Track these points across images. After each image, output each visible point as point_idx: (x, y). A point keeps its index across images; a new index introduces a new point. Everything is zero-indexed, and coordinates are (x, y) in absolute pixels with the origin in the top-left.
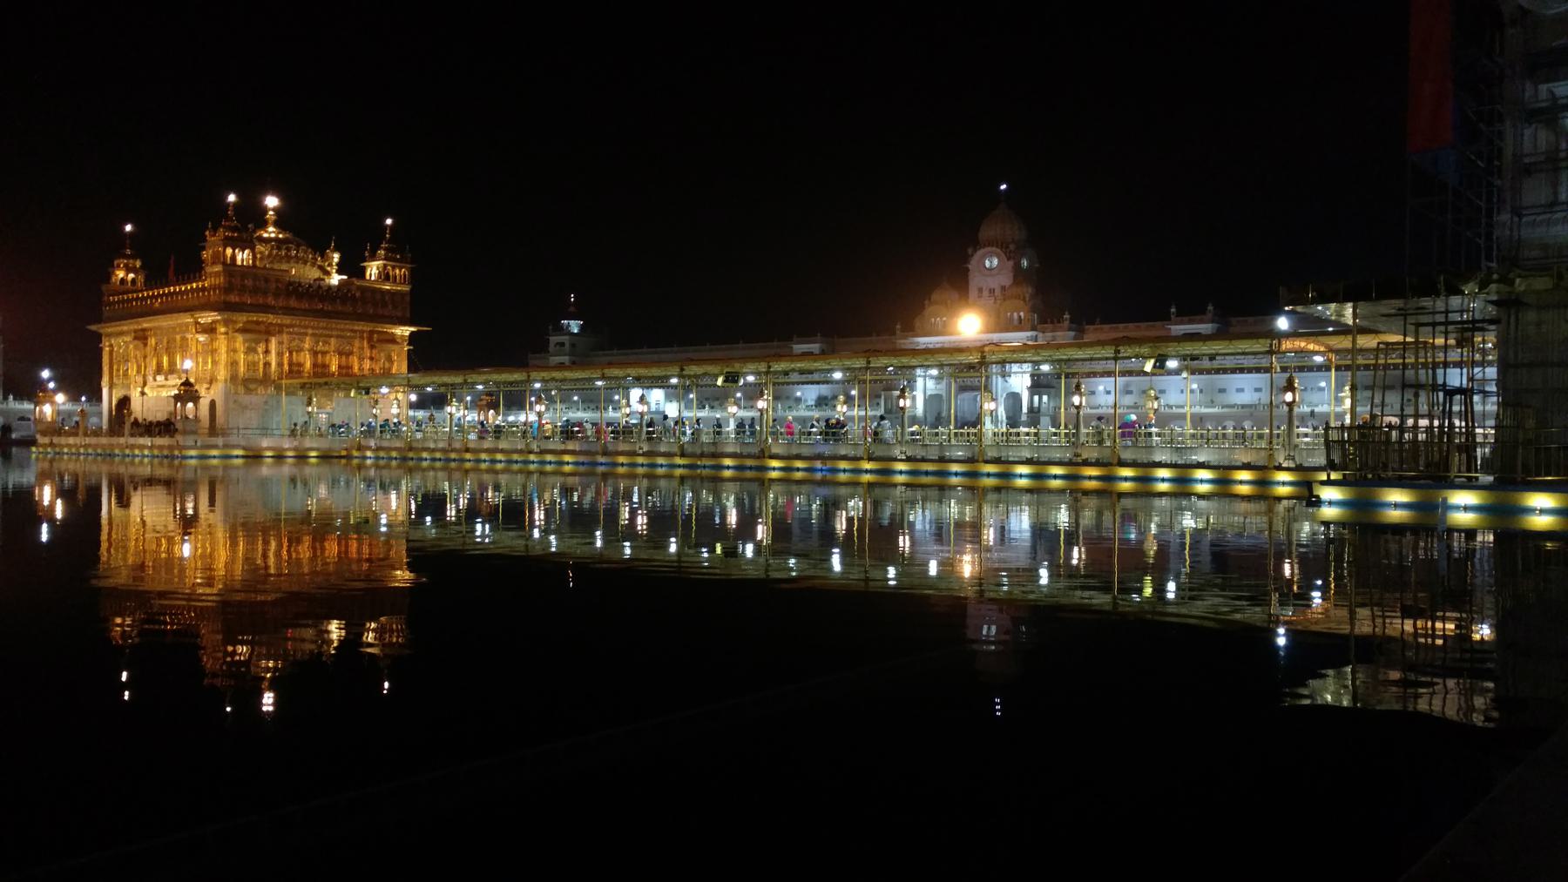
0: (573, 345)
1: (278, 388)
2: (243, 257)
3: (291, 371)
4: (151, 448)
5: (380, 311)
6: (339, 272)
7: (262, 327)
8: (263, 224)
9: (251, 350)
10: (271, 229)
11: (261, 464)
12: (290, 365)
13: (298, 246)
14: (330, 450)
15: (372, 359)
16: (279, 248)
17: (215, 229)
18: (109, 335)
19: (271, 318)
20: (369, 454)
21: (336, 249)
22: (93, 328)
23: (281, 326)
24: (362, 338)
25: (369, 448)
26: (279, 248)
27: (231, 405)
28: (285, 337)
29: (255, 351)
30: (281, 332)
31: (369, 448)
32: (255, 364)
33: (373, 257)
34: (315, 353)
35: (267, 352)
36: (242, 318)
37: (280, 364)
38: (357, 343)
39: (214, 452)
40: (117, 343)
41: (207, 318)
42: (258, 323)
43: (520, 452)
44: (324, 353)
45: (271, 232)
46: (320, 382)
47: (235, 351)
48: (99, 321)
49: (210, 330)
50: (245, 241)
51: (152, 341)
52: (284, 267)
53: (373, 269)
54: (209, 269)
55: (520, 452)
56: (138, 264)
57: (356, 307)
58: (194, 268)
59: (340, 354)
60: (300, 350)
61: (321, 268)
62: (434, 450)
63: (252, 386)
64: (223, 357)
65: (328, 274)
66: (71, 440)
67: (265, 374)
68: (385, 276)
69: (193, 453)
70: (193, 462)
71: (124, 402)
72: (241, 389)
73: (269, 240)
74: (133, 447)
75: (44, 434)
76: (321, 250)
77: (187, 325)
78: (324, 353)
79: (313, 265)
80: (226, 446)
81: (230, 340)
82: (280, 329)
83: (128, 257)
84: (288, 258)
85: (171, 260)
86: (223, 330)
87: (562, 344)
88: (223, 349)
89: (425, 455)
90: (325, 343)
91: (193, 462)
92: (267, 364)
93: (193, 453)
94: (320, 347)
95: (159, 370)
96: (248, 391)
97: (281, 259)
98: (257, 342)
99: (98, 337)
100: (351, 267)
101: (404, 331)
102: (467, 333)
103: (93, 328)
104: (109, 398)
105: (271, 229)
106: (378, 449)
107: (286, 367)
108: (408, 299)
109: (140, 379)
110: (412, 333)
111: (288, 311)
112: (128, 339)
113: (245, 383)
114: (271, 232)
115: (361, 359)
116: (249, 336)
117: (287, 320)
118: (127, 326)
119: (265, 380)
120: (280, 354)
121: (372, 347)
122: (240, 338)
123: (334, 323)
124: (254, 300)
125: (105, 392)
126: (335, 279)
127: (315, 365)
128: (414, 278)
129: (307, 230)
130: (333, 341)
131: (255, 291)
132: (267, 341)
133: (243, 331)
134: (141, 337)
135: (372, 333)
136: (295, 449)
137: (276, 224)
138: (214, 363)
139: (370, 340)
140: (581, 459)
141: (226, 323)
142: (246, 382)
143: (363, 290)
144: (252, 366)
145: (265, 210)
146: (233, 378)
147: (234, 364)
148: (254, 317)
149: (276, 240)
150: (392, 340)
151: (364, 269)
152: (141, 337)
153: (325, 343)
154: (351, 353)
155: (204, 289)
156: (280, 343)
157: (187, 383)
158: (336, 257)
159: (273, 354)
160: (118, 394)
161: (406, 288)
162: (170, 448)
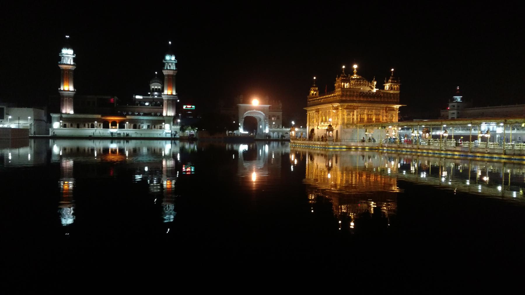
0: (458, 106)
1: (356, 126)
2: (347, 85)
3: (360, 121)
4: (320, 145)
5: (389, 100)
6: (376, 88)
7: (352, 107)
8: (352, 74)
9: (348, 115)
11: (351, 151)
12: (360, 119)
13: (363, 80)
14: (372, 147)
15: (386, 116)
17: (339, 77)
18: (309, 110)
19: (355, 104)
20: (385, 148)
22: (305, 109)
23: (358, 106)
24: (383, 109)
25: (385, 147)
26: (357, 81)
28: (359, 110)
29: (350, 115)
30: (357, 108)
31: (385, 147)
32: (349, 119)
33: (387, 82)
34: (368, 115)
35: (353, 115)
36: (346, 105)
37: (357, 119)
38: (381, 111)
39: (337, 147)
40: (311, 113)
41: (336, 105)
42: (351, 106)
43: (438, 150)
45: (355, 76)
46: (369, 124)
47: (344, 115)
48: (306, 106)
49: (337, 109)
50: (347, 81)
51: (320, 112)
52: (359, 87)
53: (387, 86)
54: (337, 90)
55: (438, 150)
56: (317, 89)
57: (381, 99)
58: (332, 89)
59: (376, 115)
60: (363, 114)
61: (371, 87)
62: (407, 148)
63: (349, 126)
64: (340, 117)
65: (372, 88)
66: (299, 142)
67: (353, 122)
68: (391, 88)
69: (331, 147)
70: (331, 150)
71: (313, 130)
72: (345, 127)
73: (355, 79)
74: (315, 144)
75: (292, 139)
76: (370, 81)
77: (330, 107)
79: (368, 86)
80: (341, 145)
81: (343, 112)
82: (357, 107)
83: (314, 87)
84: (360, 84)
85: (326, 88)
86: (340, 108)
87: (454, 106)
88: (340, 115)
89: (404, 150)
90: (371, 111)
91: (331, 150)
92: (353, 119)
93: (331, 147)
94: (370, 113)
95: (322, 121)
96: (348, 127)
97: (358, 85)
98: (350, 112)
99: (306, 111)
100: (380, 86)
101: (397, 106)
102: (419, 107)
103: (305, 109)
104: (308, 129)
105: (355, 75)
106: (388, 147)
107: (359, 120)
108: (399, 95)
109: (317, 124)
110: (400, 107)
111: (360, 102)
112: (314, 112)
113: (347, 125)
114: (355, 76)
115: (383, 116)
116: (348, 110)
117: (359, 105)
118: (313, 108)
119: (353, 124)
120: (357, 115)
121: (386, 112)
122: (345, 111)
123: (374, 105)
124: (350, 99)
125: (308, 127)
126: (375, 90)
127: (368, 119)
128: (401, 88)
129: (366, 75)
130: (374, 111)
131: (350, 96)
132: (353, 112)
133: (346, 109)
134: (317, 111)
135: (386, 107)
136: (361, 146)
137: (357, 74)
138: (338, 119)
139: (386, 110)
140: (462, 154)
141: (341, 106)
142: (347, 124)
143: (384, 93)
144: (348, 119)
145: (353, 69)
146: (343, 123)
147: (343, 119)
148: (350, 104)
149: (357, 79)
150: (393, 110)
151: (384, 86)
152: (317, 111)
153: (371, 111)
154: (380, 114)
155: (335, 96)
156: (357, 112)
157: (330, 126)
158: (375, 83)
159: (355, 116)
160: (311, 128)
161: (398, 92)
162: (325, 145)
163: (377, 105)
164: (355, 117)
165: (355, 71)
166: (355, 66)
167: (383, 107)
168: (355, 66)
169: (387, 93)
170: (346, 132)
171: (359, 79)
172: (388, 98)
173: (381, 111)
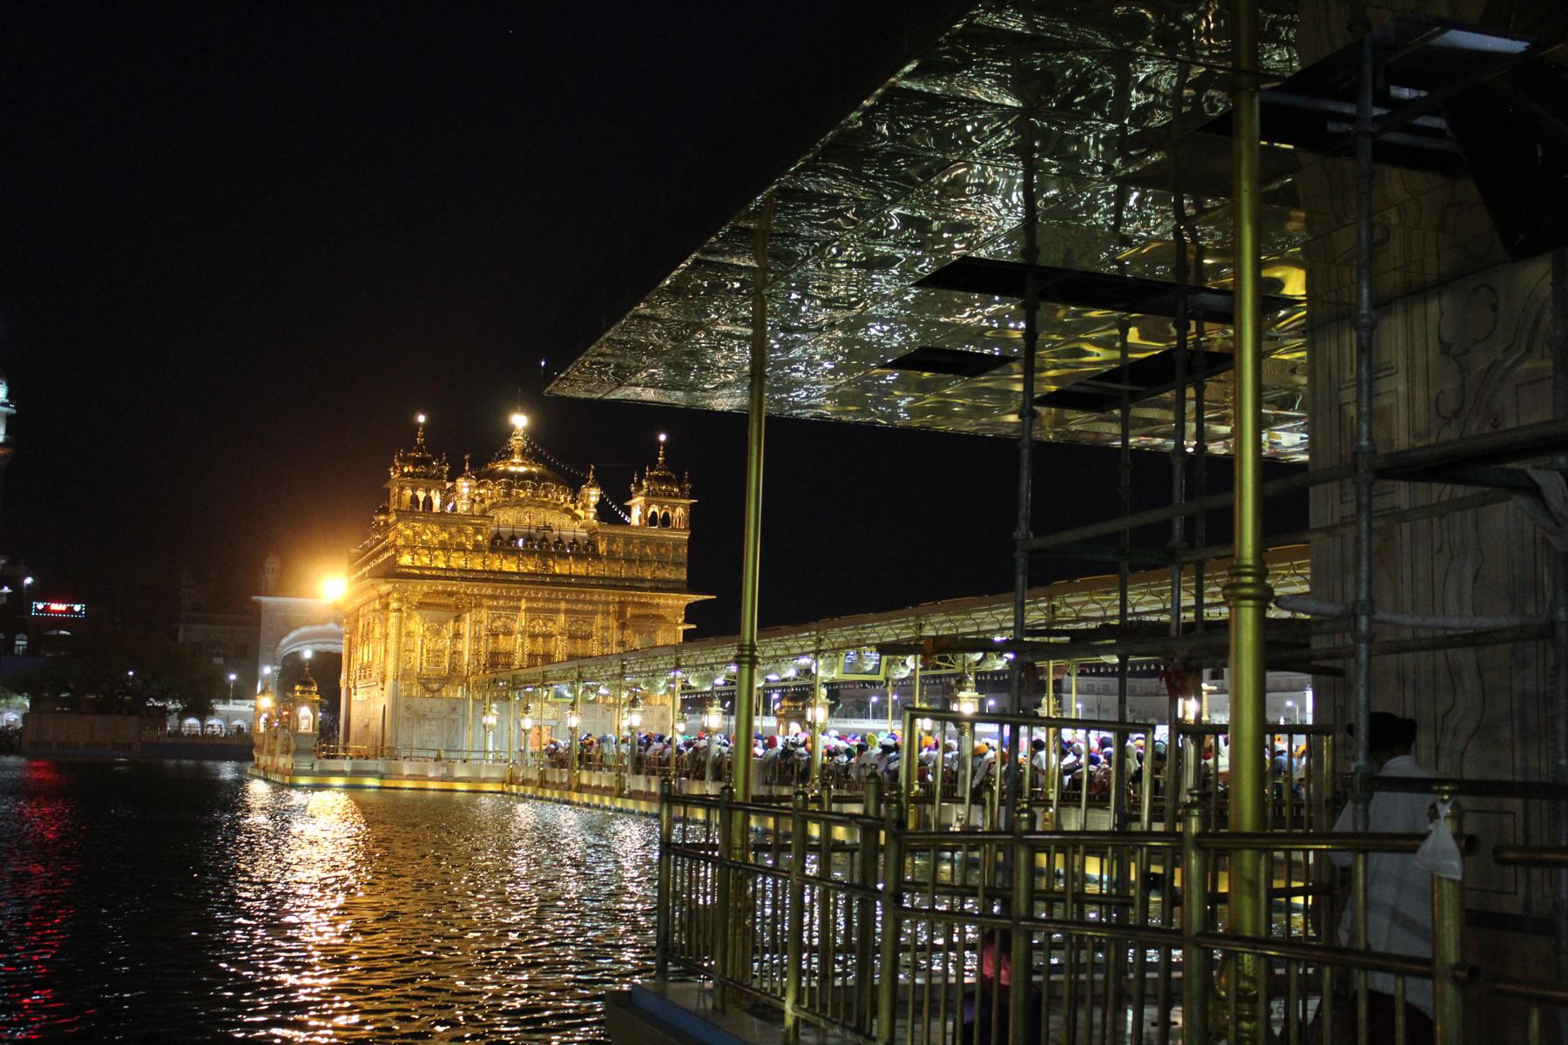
10: (517, 459)
16: (509, 486)
24: (606, 614)
26: (509, 486)
27: (402, 712)
28: (484, 613)
30: (479, 605)
37: (477, 653)
38: (599, 620)
42: (451, 594)
47: (408, 634)
64: (392, 645)
67: (454, 668)
72: (416, 690)
73: (506, 474)
76: (574, 486)
78: (548, 636)
84: (519, 503)
88: (393, 631)
92: (456, 653)
105: (517, 459)
114: (517, 466)
116: (429, 613)
120: (477, 638)
121: (623, 626)
131: (443, 547)
132: (457, 619)
133: (422, 605)
139: (620, 615)
142: (425, 682)
145: (509, 432)
158: (593, 495)
159: (467, 640)
164: (465, 646)
165: (517, 442)
167: (607, 603)
169: (628, 540)
170: (421, 717)
171: (528, 476)
172: (629, 561)
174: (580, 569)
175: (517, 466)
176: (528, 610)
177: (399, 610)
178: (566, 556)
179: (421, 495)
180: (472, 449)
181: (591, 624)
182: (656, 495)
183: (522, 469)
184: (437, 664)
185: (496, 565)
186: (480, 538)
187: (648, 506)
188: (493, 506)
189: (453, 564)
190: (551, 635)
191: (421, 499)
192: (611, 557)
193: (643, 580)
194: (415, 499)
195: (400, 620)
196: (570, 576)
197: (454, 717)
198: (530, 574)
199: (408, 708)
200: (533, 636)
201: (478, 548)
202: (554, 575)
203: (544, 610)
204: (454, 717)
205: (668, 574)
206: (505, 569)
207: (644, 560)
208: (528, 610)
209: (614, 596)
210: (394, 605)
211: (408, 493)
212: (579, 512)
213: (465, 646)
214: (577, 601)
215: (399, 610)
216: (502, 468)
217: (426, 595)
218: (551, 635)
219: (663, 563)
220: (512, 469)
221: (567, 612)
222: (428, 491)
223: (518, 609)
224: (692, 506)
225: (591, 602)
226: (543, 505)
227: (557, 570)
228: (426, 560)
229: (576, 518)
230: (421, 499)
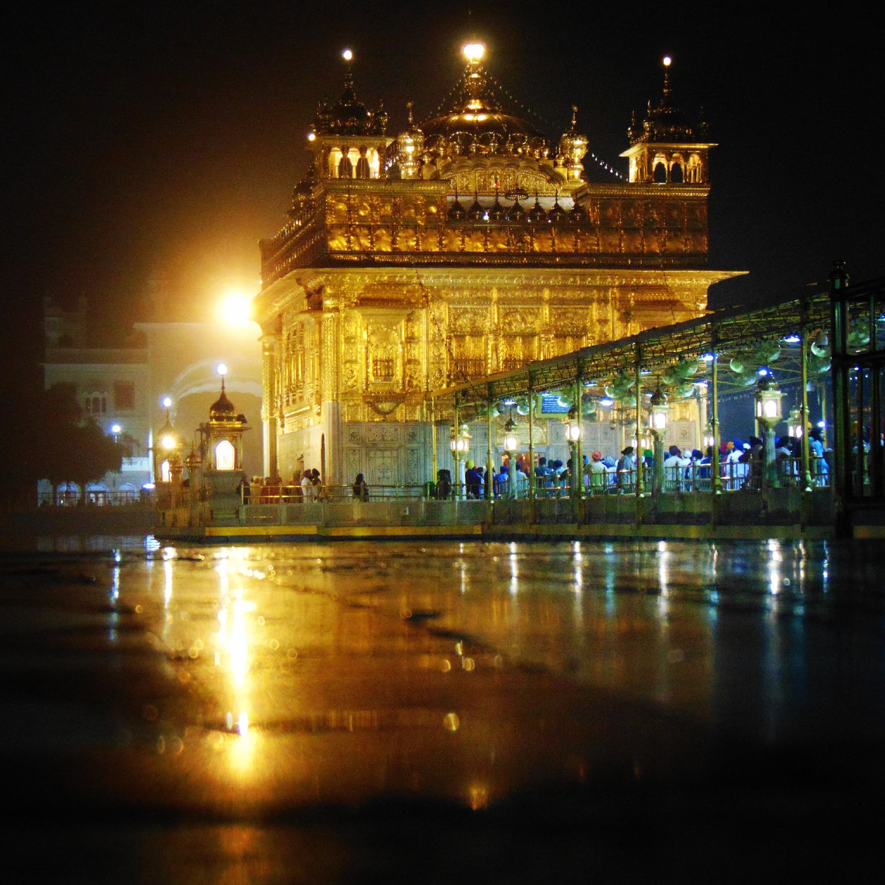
10: (475, 105)
21: (578, 132)
26: (467, 141)
27: (347, 444)
32: (388, 363)
35: (411, 339)
38: (595, 311)
44: (528, 337)
45: (475, 113)
47: (349, 340)
63: (385, 406)
72: (363, 414)
101: (703, 280)
108: (702, 213)
123: (540, 276)
133: (364, 302)
143: (605, 203)
158: (579, 147)
163: (556, 277)
166: (474, 52)
167: (606, 288)
168: (474, 52)
169: (628, 203)
172: (631, 230)
173: (595, 311)
174: (567, 246)
175: (475, 113)
176: (500, 301)
177: (336, 309)
178: (546, 229)
179: (354, 157)
180: (412, 93)
181: (584, 317)
182: (661, 139)
183: (482, 118)
184: (388, 376)
185: (457, 244)
186: (433, 209)
187: (652, 156)
188: (447, 168)
189: (402, 246)
190: (533, 335)
191: (354, 163)
192: (607, 226)
193: (652, 254)
194: (345, 164)
195: (337, 322)
196: (554, 254)
197: (414, 445)
198: (501, 254)
199: (353, 436)
200: (510, 337)
201: (433, 226)
202: (533, 254)
203: (523, 301)
204: (414, 445)
205: (684, 246)
206: (468, 249)
207: (650, 229)
208: (500, 301)
209: (615, 278)
210: (328, 303)
211: (337, 156)
212: (561, 170)
213: (421, 352)
214: (564, 287)
215: (336, 309)
216: (455, 118)
217: (367, 288)
218: (533, 335)
219: (675, 231)
220: (469, 118)
221: (551, 302)
222: (363, 150)
223: (487, 300)
224: (711, 150)
225: (583, 288)
226: (513, 164)
227: (537, 247)
228: (366, 242)
229: (556, 178)
230: (354, 163)
